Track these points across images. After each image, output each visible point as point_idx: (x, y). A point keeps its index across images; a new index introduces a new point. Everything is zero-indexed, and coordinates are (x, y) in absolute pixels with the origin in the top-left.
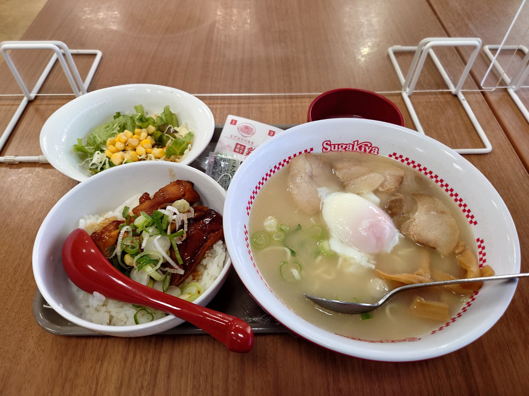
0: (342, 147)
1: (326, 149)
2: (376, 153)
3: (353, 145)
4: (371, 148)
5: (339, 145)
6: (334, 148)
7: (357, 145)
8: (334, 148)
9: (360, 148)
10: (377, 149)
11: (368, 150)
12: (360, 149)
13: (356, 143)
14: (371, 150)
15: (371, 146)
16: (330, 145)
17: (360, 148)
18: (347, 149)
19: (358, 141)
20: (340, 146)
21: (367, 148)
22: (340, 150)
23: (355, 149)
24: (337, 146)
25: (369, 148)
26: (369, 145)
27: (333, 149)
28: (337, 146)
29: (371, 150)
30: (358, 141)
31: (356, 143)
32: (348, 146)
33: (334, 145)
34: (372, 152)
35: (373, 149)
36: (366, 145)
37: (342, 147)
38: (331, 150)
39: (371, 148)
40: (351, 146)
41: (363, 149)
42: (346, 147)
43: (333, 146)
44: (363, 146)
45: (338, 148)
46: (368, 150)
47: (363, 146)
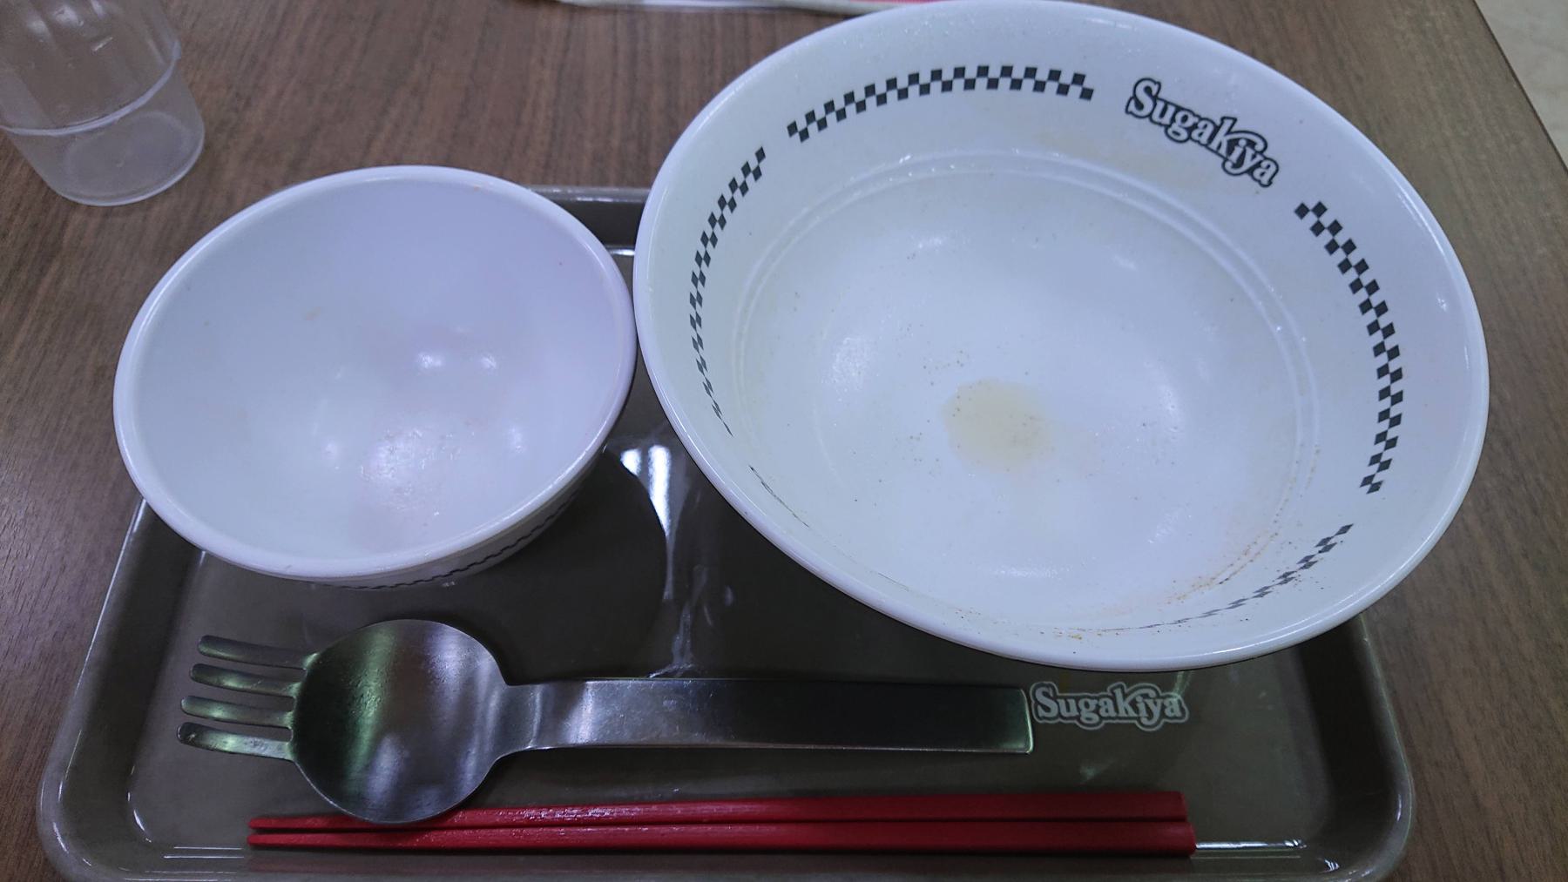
0: (1185, 119)
1: (1140, 106)
2: (1265, 180)
3: (1217, 129)
4: (1259, 158)
5: (1179, 109)
6: (1162, 115)
7: (1229, 132)
8: (1162, 115)
9: (1232, 144)
10: (1273, 168)
11: (1248, 163)
12: (1230, 151)
13: (1228, 123)
14: (1258, 165)
15: (1261, 153)
16: (1155, 99)
17: (1232, 144)
18: (1195, 134)
19: (1235, 120)
20: (1180, 116)
21: (1250, 152)
22: (1175, 127)
23: (1214, 145)
24: (1171, 110)
25: (1254, 157)
26: (1260, 146)
27: (1156, 116)
28: (1171, 110)
29: (1258, 165)
30: (1235, 120)
31: (1228, 123)
32: (1202, 124)
33: (1167, 103)
34: (1257, 173)
35: (1265, 164)
36: (1251, 144)
37: (1185, 119)
38: (1150, 116)
39: (1259, 158)
40: (1210, 128)
41: (1238, 151)
42: (1195, 126)
43: (1160, 105)
44: (1243, 143)
45: (1173, 120)
46: (1248, 163)
47: (1243, 143)
